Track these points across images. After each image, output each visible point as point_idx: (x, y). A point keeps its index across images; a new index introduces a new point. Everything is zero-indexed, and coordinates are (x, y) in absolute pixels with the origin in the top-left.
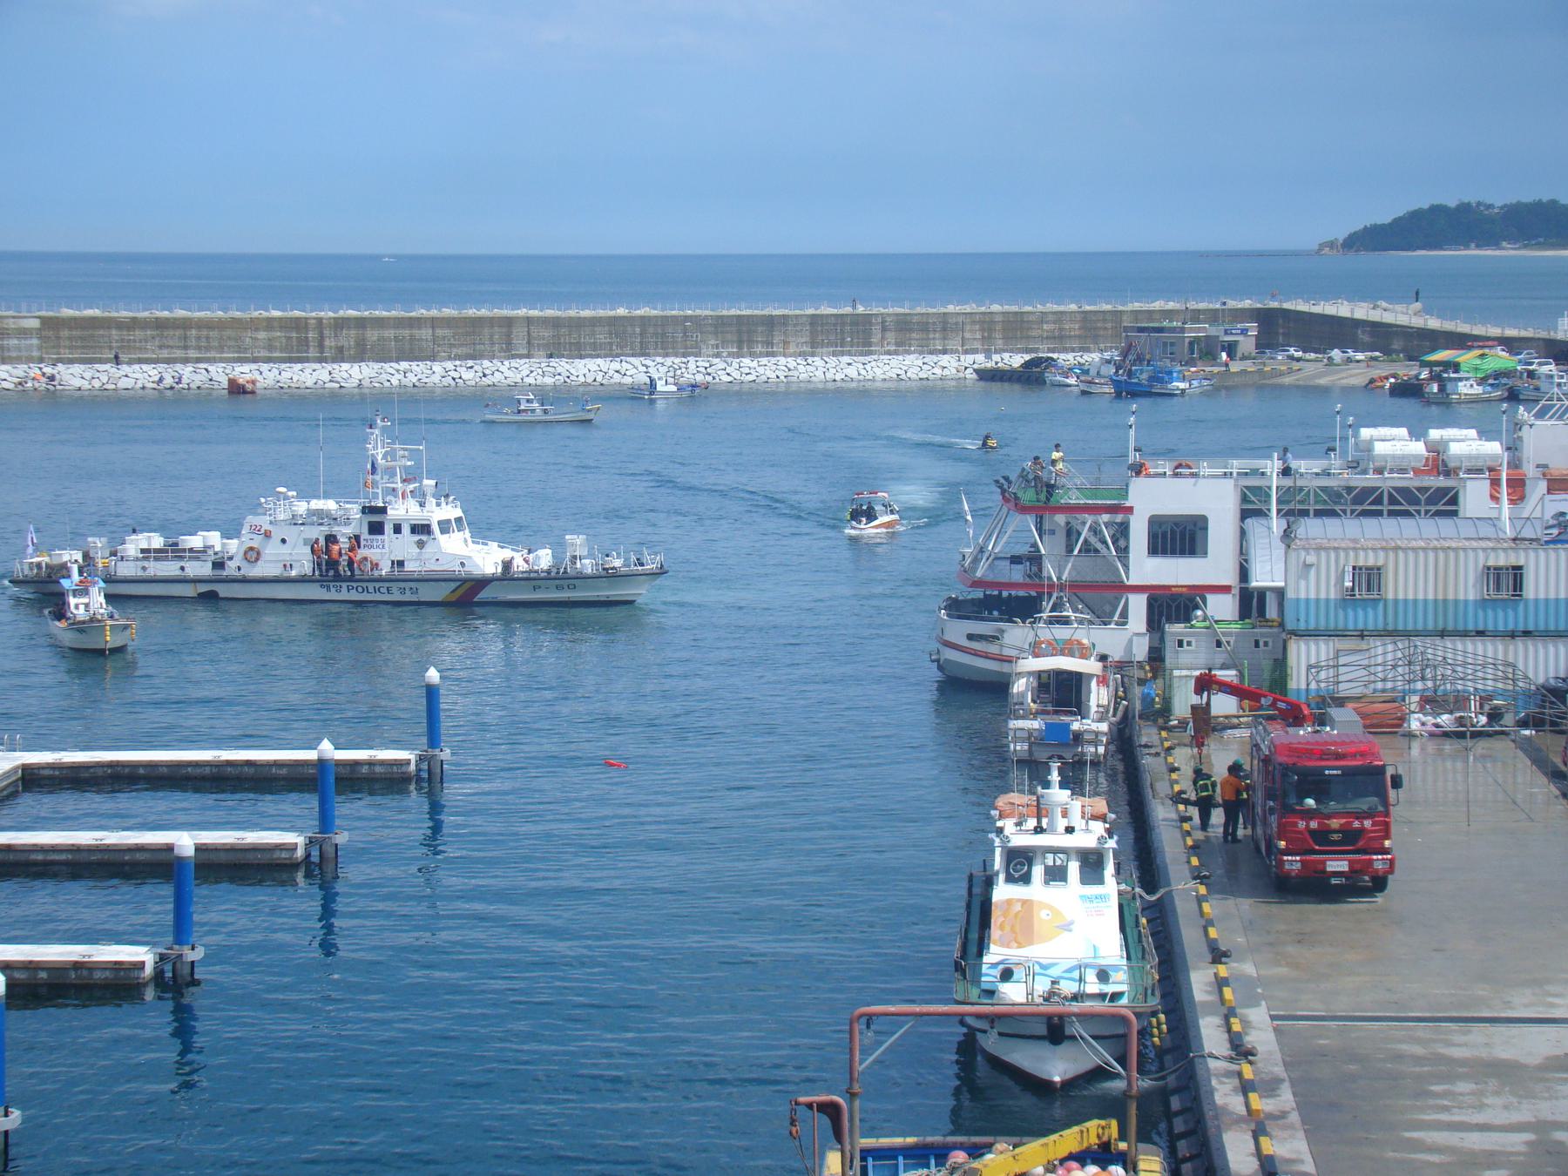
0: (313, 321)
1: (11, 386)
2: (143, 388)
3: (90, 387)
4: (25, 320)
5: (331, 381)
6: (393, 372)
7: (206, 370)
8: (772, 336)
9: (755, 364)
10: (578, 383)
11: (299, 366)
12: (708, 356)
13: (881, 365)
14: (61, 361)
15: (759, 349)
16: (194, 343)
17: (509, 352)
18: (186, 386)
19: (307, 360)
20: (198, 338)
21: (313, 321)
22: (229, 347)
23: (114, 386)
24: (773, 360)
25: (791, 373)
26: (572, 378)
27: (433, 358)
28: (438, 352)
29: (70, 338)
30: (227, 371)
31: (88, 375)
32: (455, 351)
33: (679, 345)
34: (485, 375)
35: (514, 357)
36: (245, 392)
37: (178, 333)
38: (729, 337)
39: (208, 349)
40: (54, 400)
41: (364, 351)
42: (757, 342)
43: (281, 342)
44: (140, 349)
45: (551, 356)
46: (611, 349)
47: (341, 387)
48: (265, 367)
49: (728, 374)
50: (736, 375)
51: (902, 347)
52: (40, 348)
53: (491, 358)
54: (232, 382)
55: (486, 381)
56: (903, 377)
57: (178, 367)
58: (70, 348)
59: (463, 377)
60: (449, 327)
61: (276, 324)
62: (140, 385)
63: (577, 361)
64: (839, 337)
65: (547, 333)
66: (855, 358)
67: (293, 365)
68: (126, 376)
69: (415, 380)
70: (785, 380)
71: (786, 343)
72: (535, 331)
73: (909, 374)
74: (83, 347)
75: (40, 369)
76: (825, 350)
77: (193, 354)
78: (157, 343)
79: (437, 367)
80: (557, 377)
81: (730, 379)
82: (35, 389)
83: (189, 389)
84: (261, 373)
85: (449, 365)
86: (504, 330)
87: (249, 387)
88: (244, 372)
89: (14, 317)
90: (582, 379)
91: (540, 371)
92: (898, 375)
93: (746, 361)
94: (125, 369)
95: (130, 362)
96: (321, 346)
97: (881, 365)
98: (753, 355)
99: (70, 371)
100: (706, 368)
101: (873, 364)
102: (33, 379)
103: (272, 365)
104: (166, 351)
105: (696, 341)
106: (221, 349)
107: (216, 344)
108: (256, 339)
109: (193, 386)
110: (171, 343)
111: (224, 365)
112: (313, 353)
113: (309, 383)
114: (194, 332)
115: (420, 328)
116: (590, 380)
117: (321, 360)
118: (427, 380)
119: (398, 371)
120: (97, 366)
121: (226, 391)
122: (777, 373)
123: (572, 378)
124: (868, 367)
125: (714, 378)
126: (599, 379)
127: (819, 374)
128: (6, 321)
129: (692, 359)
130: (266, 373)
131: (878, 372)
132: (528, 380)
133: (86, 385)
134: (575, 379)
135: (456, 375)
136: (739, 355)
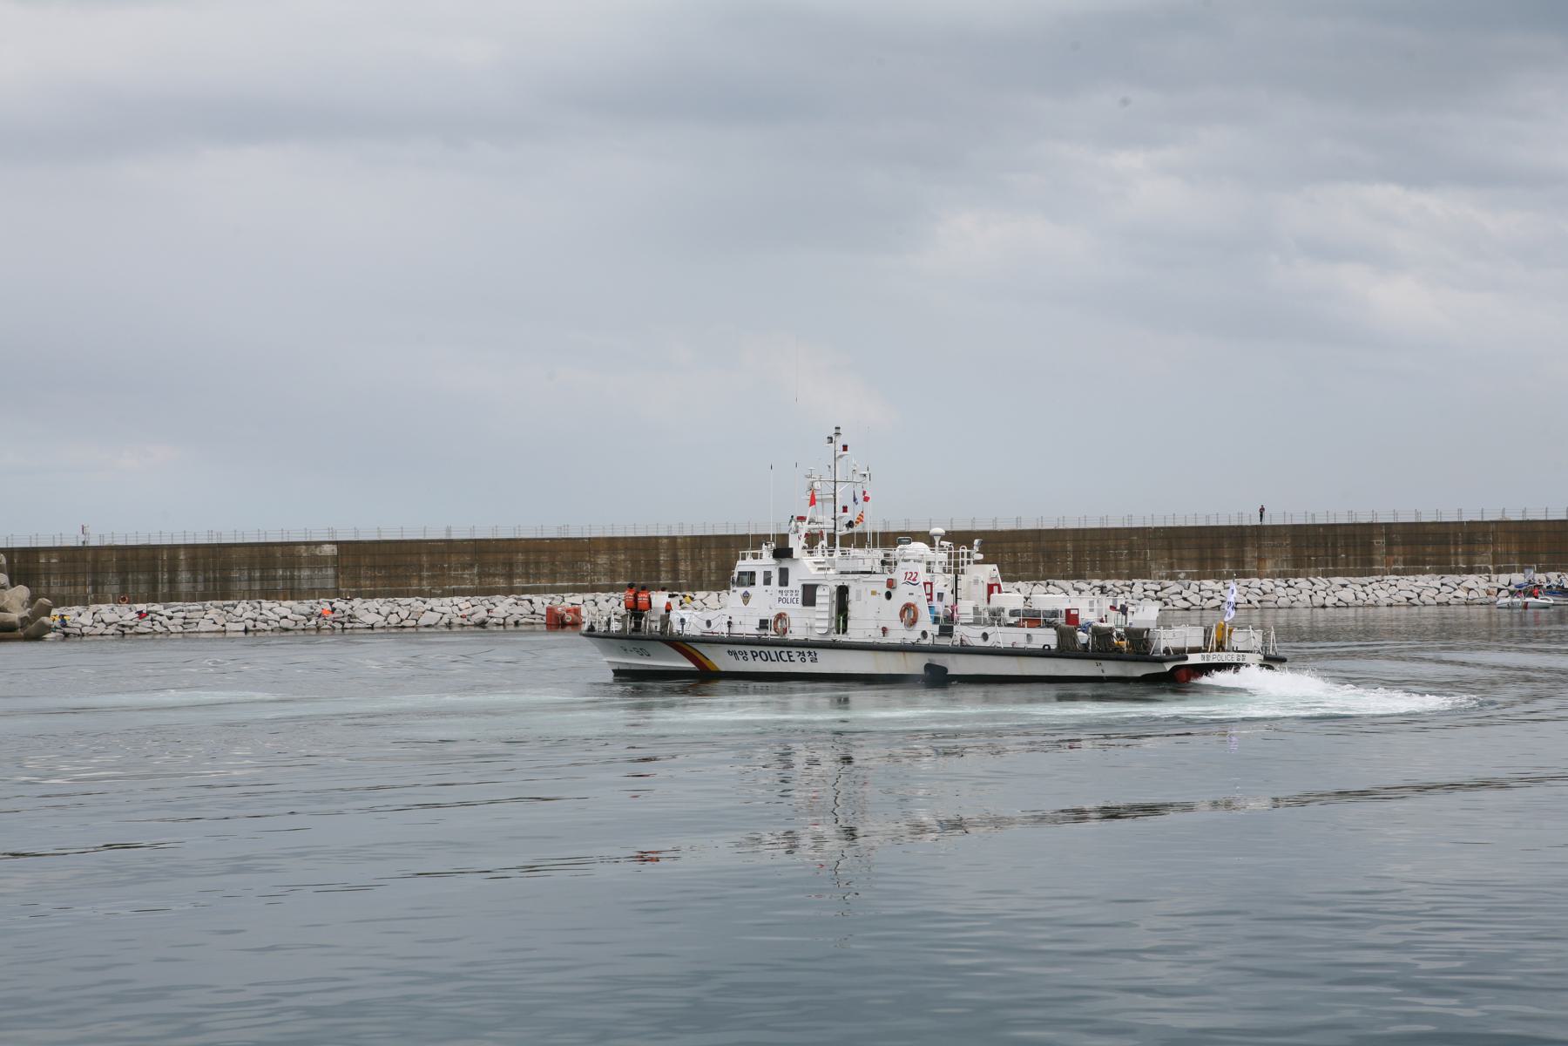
0: (665, 541)
1: (290, 625)
2: (449, 625)
7: (531, 602)
8: (1243, 551)
9: (1219, 586)
12: (1161, 578)
13: (1386, 586)
15: (1226, 569)
16: (520, 570)
18: (502, 621)
20: (526, 564)
23: (414, 623)
24: (1244, 581)
25: (1266, 597)
29: (373, 567)
30: (555, 602)
31: (385, 610)
33: (1124, 564)
37: (501, 557)
38: (1186, 553)
39: (537, 576)
42: (1224, 559)
43: (626, 568)
44: (456, 578)
46: (1037, 570)
48: (601, 597)
49: (1185, 599)
50: (1195, 599)
51: (1414, 565)
52: (337, 577)
56: (1416, 601)
57: (497, 598)
58: (373, 578)
61: (620, 545)
62: (446, 620)
64: (1330, 551)
66: (1351, 579)
68: (432, 610)
70: (1258, 605)
71: (1260, 559)
73: (1422, 598)
75: (331, 604)
76: (1312, 570)
77: (518, 583)
81: (1187, 605)
83: (504, 625)
84: (596, 604)
87: (569, 618)
89: (307, 544)
92: (1408, 599)
93: (1209, 584)
94: (433, 602)
96: (675, 572)
97: (1386, 586)
98: (1217, 576)
100: (1156, 592)
101: (1375, 585)
102: (320, 616)
103: (611, 594)
105: (1145, 559)
106: (553, 575)
109: (510, 620)
111: (552, 595)
114: (520, 557)
122: (1249, 597)
124: (1369, 589)
125: (1166, 604)
127: (1304, 597)
128: (297, 548)
129: (1138, 582)
130: (602, 604)
131: (1382, 595)
133: (380, 621)
136: (1200, 577)
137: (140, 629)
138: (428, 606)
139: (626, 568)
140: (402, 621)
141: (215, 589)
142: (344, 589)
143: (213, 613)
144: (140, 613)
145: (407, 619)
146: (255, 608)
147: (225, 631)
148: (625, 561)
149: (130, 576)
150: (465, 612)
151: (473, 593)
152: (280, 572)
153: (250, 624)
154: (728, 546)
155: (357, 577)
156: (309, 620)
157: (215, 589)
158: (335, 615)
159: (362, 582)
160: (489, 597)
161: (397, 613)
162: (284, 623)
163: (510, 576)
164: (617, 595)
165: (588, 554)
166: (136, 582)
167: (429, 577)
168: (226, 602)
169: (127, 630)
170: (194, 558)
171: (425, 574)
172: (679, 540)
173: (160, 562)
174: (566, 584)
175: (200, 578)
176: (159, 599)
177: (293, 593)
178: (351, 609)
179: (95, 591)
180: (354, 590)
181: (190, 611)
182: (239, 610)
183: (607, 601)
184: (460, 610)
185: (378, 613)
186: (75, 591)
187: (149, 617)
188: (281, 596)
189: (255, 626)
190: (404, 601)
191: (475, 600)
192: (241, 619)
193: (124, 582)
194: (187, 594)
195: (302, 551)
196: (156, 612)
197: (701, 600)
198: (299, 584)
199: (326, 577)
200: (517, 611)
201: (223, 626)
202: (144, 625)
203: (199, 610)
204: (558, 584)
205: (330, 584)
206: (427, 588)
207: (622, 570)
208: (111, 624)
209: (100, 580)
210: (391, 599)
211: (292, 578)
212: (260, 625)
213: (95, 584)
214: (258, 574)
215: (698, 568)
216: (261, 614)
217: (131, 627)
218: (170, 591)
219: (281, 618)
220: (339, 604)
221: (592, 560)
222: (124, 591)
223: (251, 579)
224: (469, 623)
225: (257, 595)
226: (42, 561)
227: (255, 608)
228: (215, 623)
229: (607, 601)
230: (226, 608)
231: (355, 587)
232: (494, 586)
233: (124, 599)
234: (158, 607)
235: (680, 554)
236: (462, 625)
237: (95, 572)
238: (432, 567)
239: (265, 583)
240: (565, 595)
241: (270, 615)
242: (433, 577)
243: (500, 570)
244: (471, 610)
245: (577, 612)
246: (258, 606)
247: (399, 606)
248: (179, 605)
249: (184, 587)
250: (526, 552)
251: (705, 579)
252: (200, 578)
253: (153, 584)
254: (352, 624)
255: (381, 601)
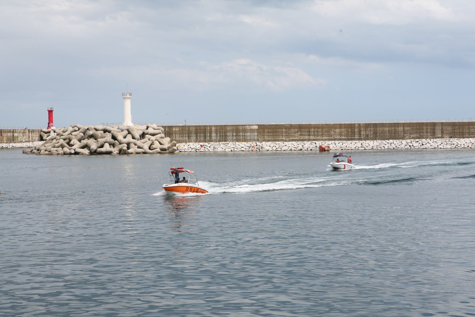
0: (357, 125)
2: (291, 150)
3: (272, 149)
4: (253, 126)
5: (361, 147)
6: (386, 143)
7: (315, 143)
10: (462, 147)
11: (351, 142)
14: (264, 140)
16: (312, 134)
17: (434, 136)
19: (354, 139)
20: (314, 132)
21: (357, 125)
22: (325, 135)
26: (458, 145)
27: (403, 138)
28: (405, 136)
29: (268, 132)
30: (323, 144)
31: (272, 146)
32: (412, 136)
34: (423, 145)
35: (436, 138)
36: (325, 151)
37: (307, 130)
39: (318, 136)
40: (260, 153)
41: (376, 136)
43: (345, 133)
45: (451, 137)
47: (365, 149)
52: (258, 135)
53: (426, 138)
54: (321, 147)
55: (423, 147)
57: (305, 142)
58: (268, 136)
59: (414, 145)
60: (410, 126)
61: (343, 126)
63: (461, 139)
65: (449, 128)
67: (348, 141)
68: (286, 146)
69: (394, 146)
72: (444, 128)
74: (273, 136)
75: (256, 143)
77: (312, 137)
78: (299, 134)
79: (404, 142)
80: (452, 145)
82: (252, 151)
83: (307, 150)
85: (409, 141)
86: (432, 127)
87: (326, 149)
88: (325, 144)
89: (249, 125)
90: (463, 146)
91: (445, 143)
94: (286, 143)
95: (289, 141)
96: (360, 134)
99: (266, 144)
103: (340, 141)
104: (302, 137)
106: (322, 135)
107: (320, 134)
108: (335, 132)
110: (304, 134)
111: (322, 141)
112: (357, 137)
113: (353, 148)
114: (312, 130)
115: (398, 127)
116: (466, 146)
117: (360, 139)
118: (399, 147)
119: (388, 143)
120: (276, 142)
121: (319, 151)
123: (458, 145)
126: (470, 146)
128: (246, 126)
130: (337, 144)
132: (440, 146)
133: (270, 149)
134: (460, 146)
135: (411, 145)
137: (201, 150)
138: (284, 144)
139: (345, 133)
140: (277, 149)
141: (223, 138)
142: (260, 139)
143: (222, 146)
144: (201, 145)
145: (278, 148)
146: (234, 144)
147: (225, 151)
148: (344, 131)
149: (198, 135)
150: (296, 146)
151: (298, 140)
152: (241, 134)
153: (233, 149)
154: (377, 127)
155: (264, 135)
156: (250, 148)
157: (223, 138)
158: (257, 147)
159: (265, 137)
160: (303, 142)
161: (275, 146)
162: (242, 149)
163: (309, 135)
164: (342, 142)
165: (333, 129)
166: (200, 136)
167: (285, 136)
168: (226, 143)
169: (197, 150)
170: (216, 129)
171: (284, 134)
172: (361, 125)
173: (207, 130)
174: (326, 138)
175: (218, 135)
176: (207, 141)
177: (245, 140)
178: (262, 145)
179: (189, 139)
180: (263, 139)
181: (215, 145)
182: (229, 145)
183: (339, 143)
184: (294, 146)
185: (270, 146)
186: (183, 139)
187: (204, 147)
188: (242, 141)
189: (234, 150)
190: (277, 143)
191: (299, 142)
192: (230, 148)
193: (197, 136)
194: (214, 140)
195: (248, 127)
196: (206, 145)
197: (368, 143)
198: (247, 137)
199: (255, 135)
200: (311, 146)
201: (225, 149)
202: (202, 149)
203: (218, 145)
204: (324, 138)
205: (256, 138)
206: (284, 139)
207: (344, 134)
208: (193, 149)
209: (190, 136)
210: (274, 142)
211: (245, 135)
212: (235, 150)
213: (189, 137)
214: (235, 134)
215: (367, 133)
216: (236, 146)
217: (199, 150)
218: (210, 139)
219: (242, 147)
220: (258, 144)
221: (334, 131)
222: (197, 139)
223: (233, 136)
224: (297, 150)
225: (235, 140)
226: (174, 130)
227: (234, 144)
228: (222, 149)
229: (339, 143)
230: (226, 144)
231: (263, 138)
232: (304, 138)
233: (197, 141)
234: (206, 144)
235: (361, 129)
236: (295, 150)
237: (189, 133)
238: (286, 132)
239: (237, 137)
240: (326, 141)
241: (238, 146)
242: (286, 135)
243: (306, 134)
244: (298, 146)
245: (329, 147)
246: (235, 144)
247: (276, 144)
248: (212, 143)
249: (214, 138)
250: (314, 128)
251: (369, 137)
252: (218, 135)
253: (205, 137)
254: (262, 150)
255: (271, 142)
